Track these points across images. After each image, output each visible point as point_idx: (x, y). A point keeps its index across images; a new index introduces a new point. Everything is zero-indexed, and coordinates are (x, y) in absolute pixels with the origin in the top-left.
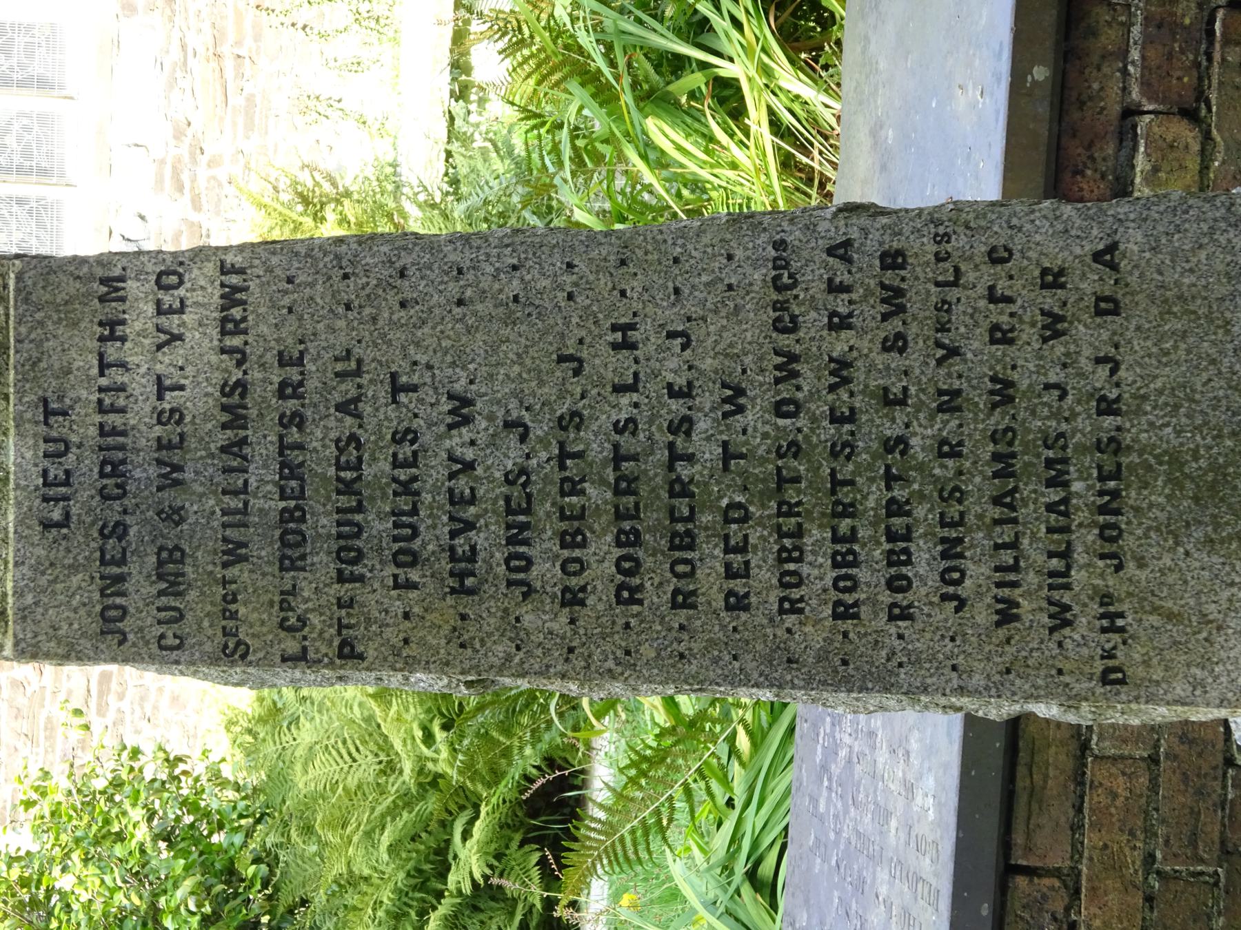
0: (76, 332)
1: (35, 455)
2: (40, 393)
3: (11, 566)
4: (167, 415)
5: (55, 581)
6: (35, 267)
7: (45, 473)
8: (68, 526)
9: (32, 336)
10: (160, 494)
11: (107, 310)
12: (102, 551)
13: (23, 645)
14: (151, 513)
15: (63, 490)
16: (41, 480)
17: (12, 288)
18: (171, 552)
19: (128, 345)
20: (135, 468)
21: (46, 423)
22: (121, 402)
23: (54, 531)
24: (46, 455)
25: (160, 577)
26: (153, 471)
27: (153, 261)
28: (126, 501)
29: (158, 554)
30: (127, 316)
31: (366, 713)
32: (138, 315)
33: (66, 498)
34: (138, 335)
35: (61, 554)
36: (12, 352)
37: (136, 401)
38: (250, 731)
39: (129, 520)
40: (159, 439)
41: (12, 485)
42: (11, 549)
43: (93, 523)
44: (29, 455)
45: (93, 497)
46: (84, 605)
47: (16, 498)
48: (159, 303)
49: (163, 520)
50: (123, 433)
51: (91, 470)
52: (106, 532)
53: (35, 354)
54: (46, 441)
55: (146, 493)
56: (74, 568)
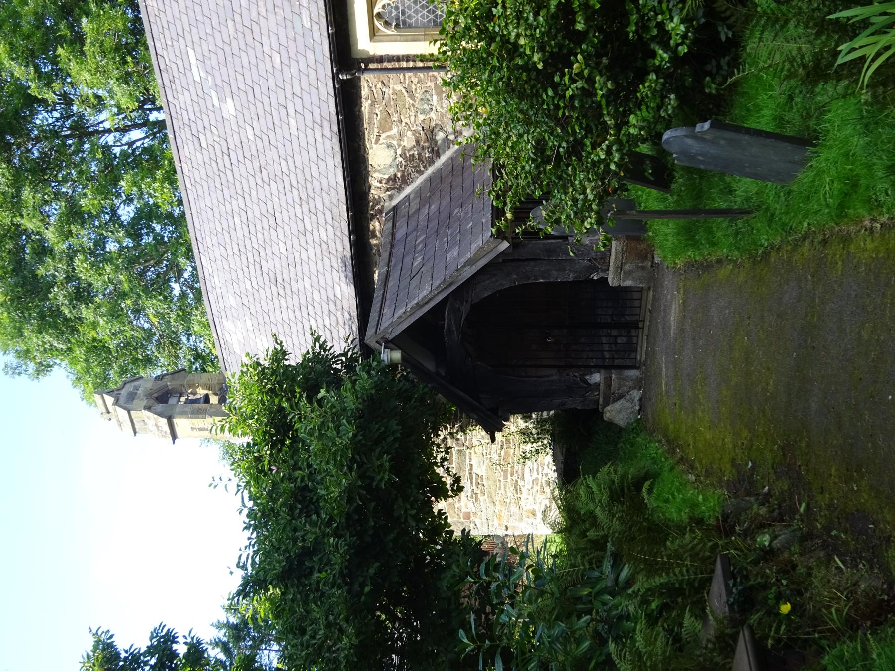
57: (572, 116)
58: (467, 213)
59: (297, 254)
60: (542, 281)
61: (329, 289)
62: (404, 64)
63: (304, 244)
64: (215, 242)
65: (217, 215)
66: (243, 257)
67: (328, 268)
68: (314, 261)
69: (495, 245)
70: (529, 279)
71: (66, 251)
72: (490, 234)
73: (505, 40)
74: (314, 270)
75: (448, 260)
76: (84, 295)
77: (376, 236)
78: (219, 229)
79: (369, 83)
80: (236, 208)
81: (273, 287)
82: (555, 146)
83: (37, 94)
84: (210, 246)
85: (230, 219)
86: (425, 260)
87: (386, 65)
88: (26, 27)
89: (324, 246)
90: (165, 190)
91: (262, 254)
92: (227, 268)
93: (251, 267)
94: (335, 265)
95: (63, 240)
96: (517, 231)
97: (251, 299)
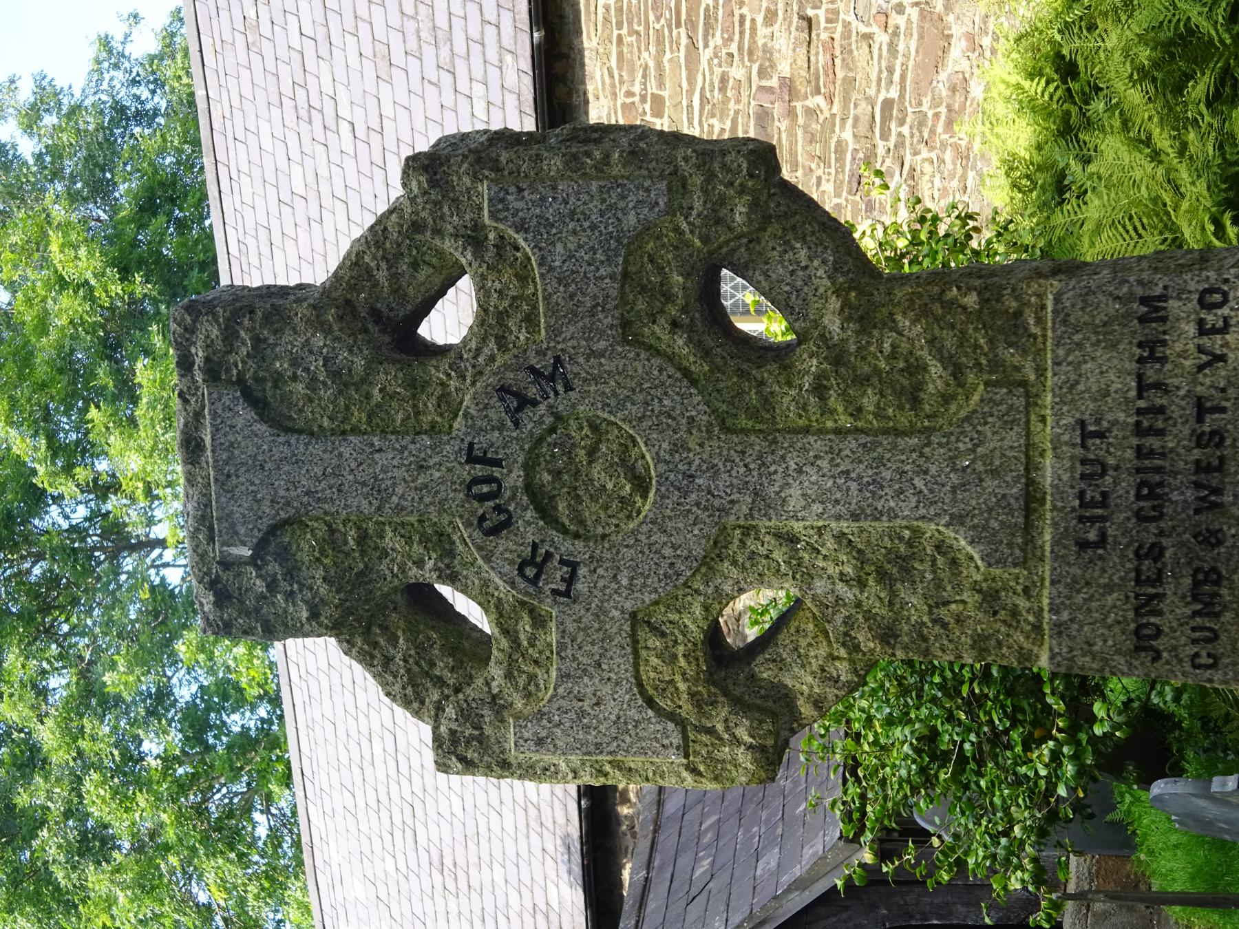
0: (1115, 354)
1: (1072, 478)
2: (1078, 415)
3: (1047, 583)
4: (1206, 438)
5: (1091, 599)
6: (1074, 288)
7: (1081, 495)
8: (1104, 548)
9: (1070, 358)
10: (1197, 517)
11: (1147, 331)
12: (1138, 571)
13: (1059, 658)
14: (1187, 536)
15: (1099, 511)
16: (1077, 503)
17: (1050, 309)
18: (1207, 574)
19: (1168, 366)
20: (1172, 491)
21: (1083, 446)
22: (1160, 424)
23: (1090, 552)
24: (1083, 476)
25: (1196, 598)
26: (1190, 494)
27: (1196, 278)
28: (1163, 525)
29: (1194, 576)
30: (1167, 337)
31: (1153, 194)
32: (1179, 336)
33: (1103, 519)
34: (1179, 356)
35: (1097, 574)
36: (1049, 374)
37: (1175, 425)
38: (1028, 177)
39: (1165, 542)
40: (1198, 462)
41: (1048, 506)
42: (1047, 567)
43: (1128, 546)
44: (1066, 477)
45: (1128, 519)
46: (1119, 623)
47: (1053, 519)
48: (1201, 323)
49: (1200, 543)
50: (1163, 455)
51: (1128, 492)
52: (1142, 552)
53: (1073, 377)
54: (1083, 462)
55: (1183, 516)
56: (1109, 588)
57: (987, 695)
58: (796, 783)
59: (482, 821)
60: (935, 922)
61: (537, 890)
63: (496, 803)
64: (335, 782)
65: (342, 734)
66: (384, 815)
67: (537, 851)
68: (513, 835)
69: (847, 854)
70: (911, 917)
71: (72, 764)
72: (838, 834)
74: (511, 853)
75: (758, 873)
76: (94, 847)
77: (629, 801)
78: (344, 760)
80: (376, 727)
81: (436, 874)
82: (955, 742)
83: (46, 485)
84: (326, 788)
85: (365, 743)
86: (717, 866)
88: (41, 371)
89: (532, 812)
90: (256, 662)
91: (419, 812)
92: (353, 829)
93: (398, 834)
94: (550, 847)
95: (68, 744)
96: (885, 869)
97: (394, 892)
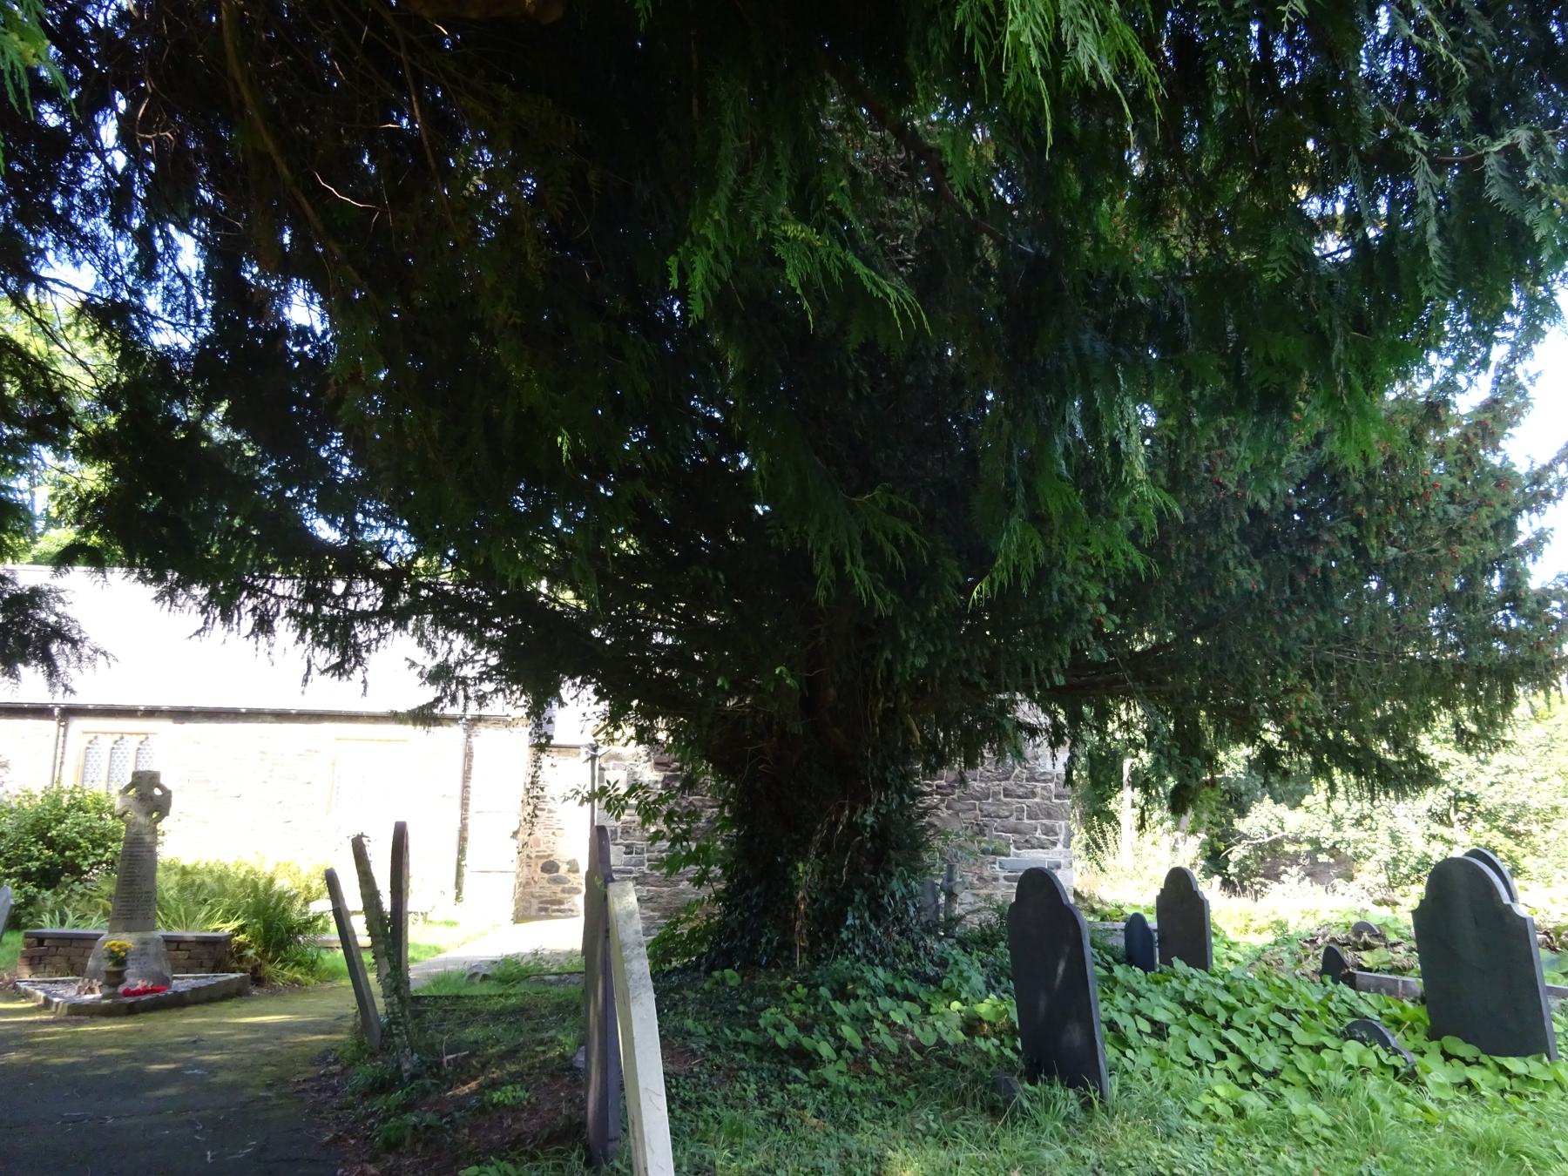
62: (60, 750)
73: (65, 817)
79: (49, 726)
87: (61, 739)
